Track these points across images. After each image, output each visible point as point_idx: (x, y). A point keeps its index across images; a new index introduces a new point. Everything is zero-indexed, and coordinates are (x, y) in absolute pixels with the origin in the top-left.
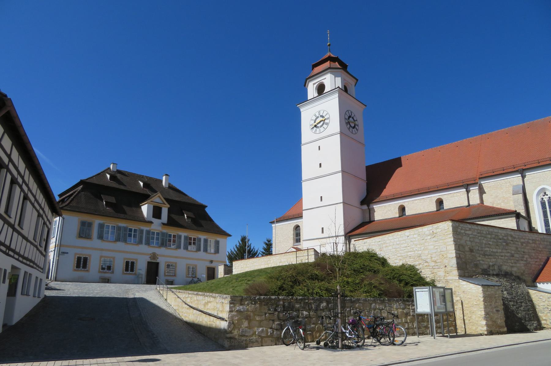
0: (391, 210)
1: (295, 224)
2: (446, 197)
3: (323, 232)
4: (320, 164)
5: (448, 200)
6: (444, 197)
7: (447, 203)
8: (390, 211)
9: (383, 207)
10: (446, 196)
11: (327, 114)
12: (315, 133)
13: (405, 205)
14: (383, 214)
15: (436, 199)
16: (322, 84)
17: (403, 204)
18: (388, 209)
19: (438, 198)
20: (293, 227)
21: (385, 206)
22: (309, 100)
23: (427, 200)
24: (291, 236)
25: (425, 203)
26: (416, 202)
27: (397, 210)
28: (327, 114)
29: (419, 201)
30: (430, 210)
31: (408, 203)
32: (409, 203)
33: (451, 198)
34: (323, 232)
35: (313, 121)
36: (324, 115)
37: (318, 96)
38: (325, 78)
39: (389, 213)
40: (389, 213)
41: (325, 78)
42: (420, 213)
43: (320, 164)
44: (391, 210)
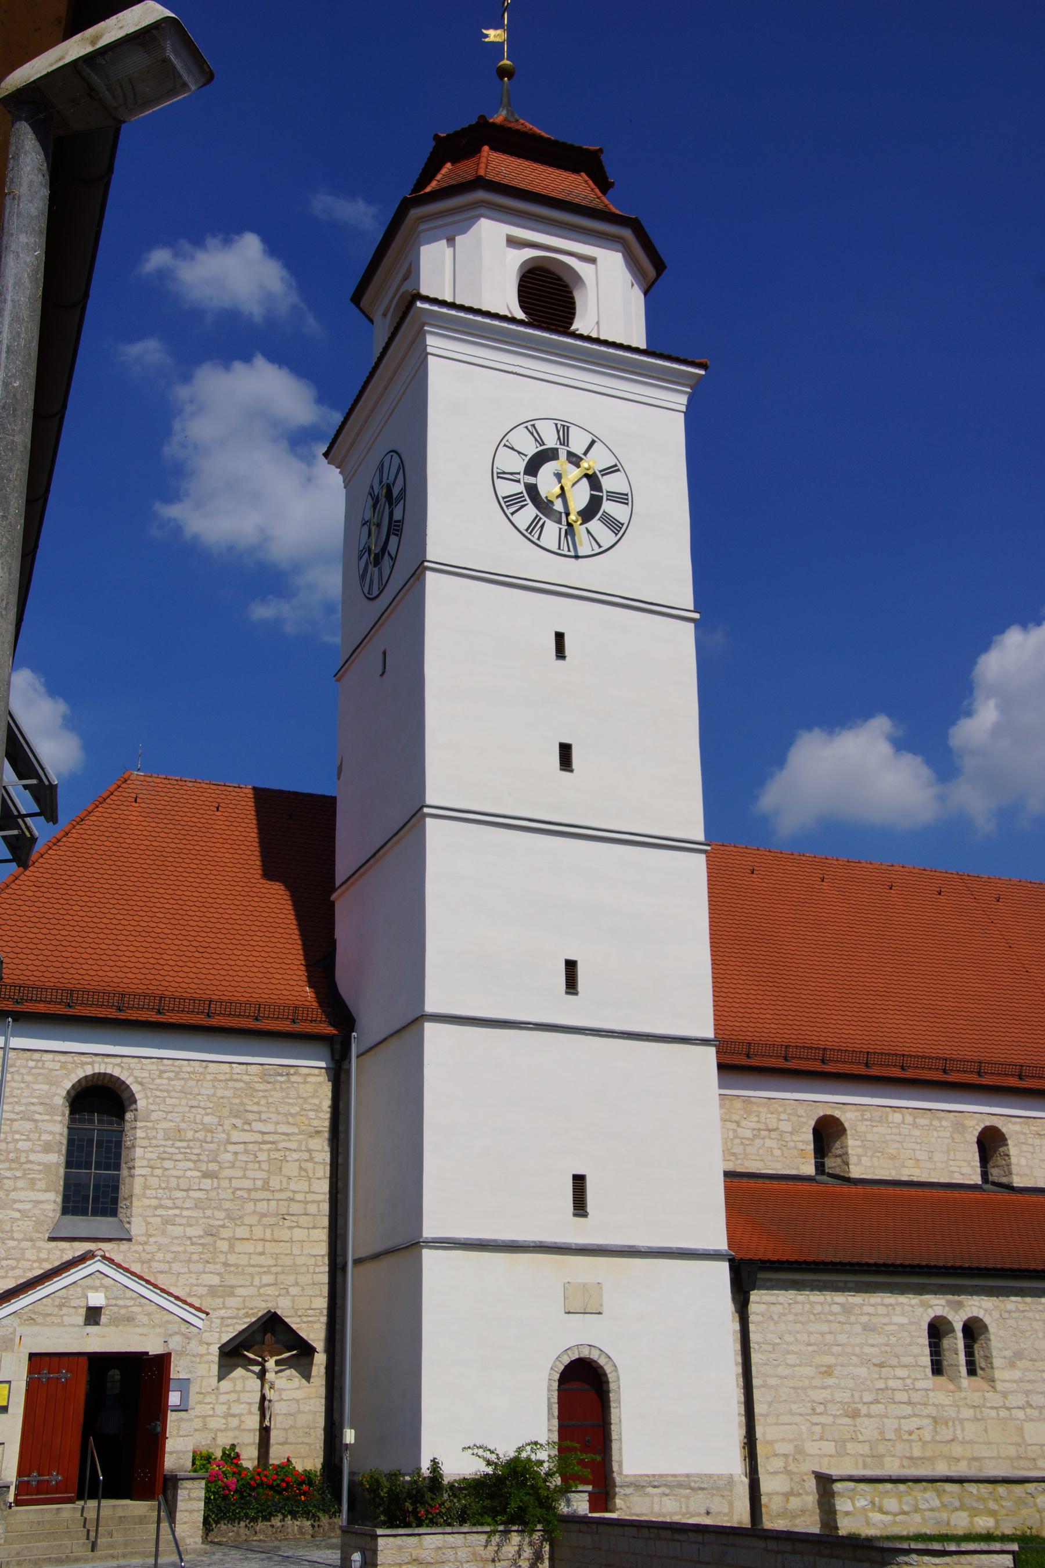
0: (778, 1128)
1: (89, 1071)
2: (1017, 1128)
3: (580, 1206)
4: (565, 753)
5: (1025, 1147)
6: (1010, 1125)
7: (1023, 1162)
8: (774, 1135)
9: (738, 1104)
10: (1014, 1123)
11: (612, 470)
12: (532, 533)
13: (847, 1118)
14: (737, 1141)
15: (980, 1129)
16: (560, 279)
17: (837, 1114)
18: (763, 1120)
19: (988, 1124)
20: (68, 1085)
21: (747, 1100)
22: (581, 337)
23: (944, 1123)
24: (32, 1157)
25: (935, 1134)
26: (897, 1117)
27: (806, 1138)
28: (612, 470)
29: (909, 1119)
30: (957, 1175)
31: (858, 1114)
32: (867, 1115)
33: (1037, 1142)
34: (580, 1206)
35: (520, 465)
36: (531, 449)
37: (520, 322)
38: (592, 260)
39: (769, 1143)
40: (769, 1143)
41: (592, 260)
42: (915, 1179)
43: (565, 753)
44: (778, 1128)
